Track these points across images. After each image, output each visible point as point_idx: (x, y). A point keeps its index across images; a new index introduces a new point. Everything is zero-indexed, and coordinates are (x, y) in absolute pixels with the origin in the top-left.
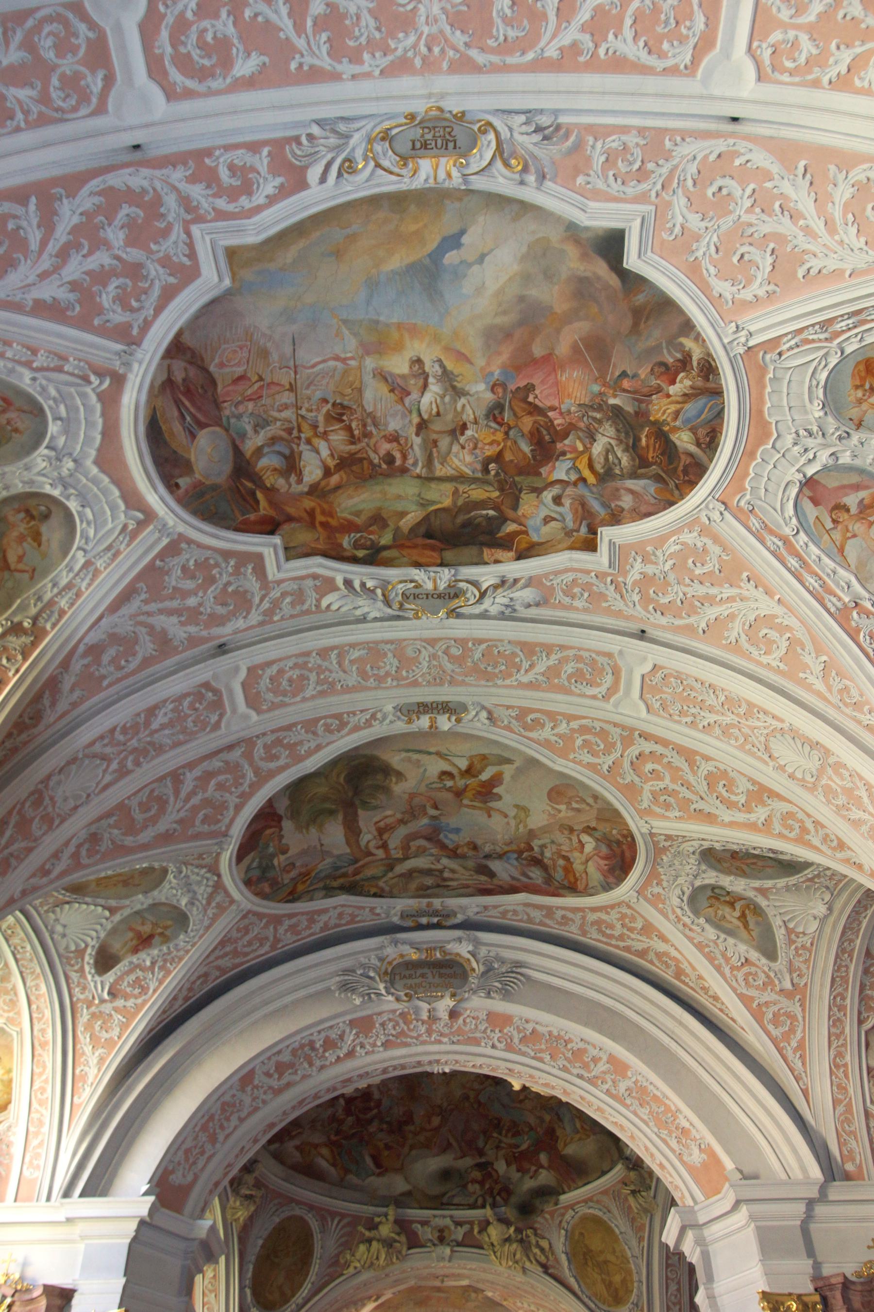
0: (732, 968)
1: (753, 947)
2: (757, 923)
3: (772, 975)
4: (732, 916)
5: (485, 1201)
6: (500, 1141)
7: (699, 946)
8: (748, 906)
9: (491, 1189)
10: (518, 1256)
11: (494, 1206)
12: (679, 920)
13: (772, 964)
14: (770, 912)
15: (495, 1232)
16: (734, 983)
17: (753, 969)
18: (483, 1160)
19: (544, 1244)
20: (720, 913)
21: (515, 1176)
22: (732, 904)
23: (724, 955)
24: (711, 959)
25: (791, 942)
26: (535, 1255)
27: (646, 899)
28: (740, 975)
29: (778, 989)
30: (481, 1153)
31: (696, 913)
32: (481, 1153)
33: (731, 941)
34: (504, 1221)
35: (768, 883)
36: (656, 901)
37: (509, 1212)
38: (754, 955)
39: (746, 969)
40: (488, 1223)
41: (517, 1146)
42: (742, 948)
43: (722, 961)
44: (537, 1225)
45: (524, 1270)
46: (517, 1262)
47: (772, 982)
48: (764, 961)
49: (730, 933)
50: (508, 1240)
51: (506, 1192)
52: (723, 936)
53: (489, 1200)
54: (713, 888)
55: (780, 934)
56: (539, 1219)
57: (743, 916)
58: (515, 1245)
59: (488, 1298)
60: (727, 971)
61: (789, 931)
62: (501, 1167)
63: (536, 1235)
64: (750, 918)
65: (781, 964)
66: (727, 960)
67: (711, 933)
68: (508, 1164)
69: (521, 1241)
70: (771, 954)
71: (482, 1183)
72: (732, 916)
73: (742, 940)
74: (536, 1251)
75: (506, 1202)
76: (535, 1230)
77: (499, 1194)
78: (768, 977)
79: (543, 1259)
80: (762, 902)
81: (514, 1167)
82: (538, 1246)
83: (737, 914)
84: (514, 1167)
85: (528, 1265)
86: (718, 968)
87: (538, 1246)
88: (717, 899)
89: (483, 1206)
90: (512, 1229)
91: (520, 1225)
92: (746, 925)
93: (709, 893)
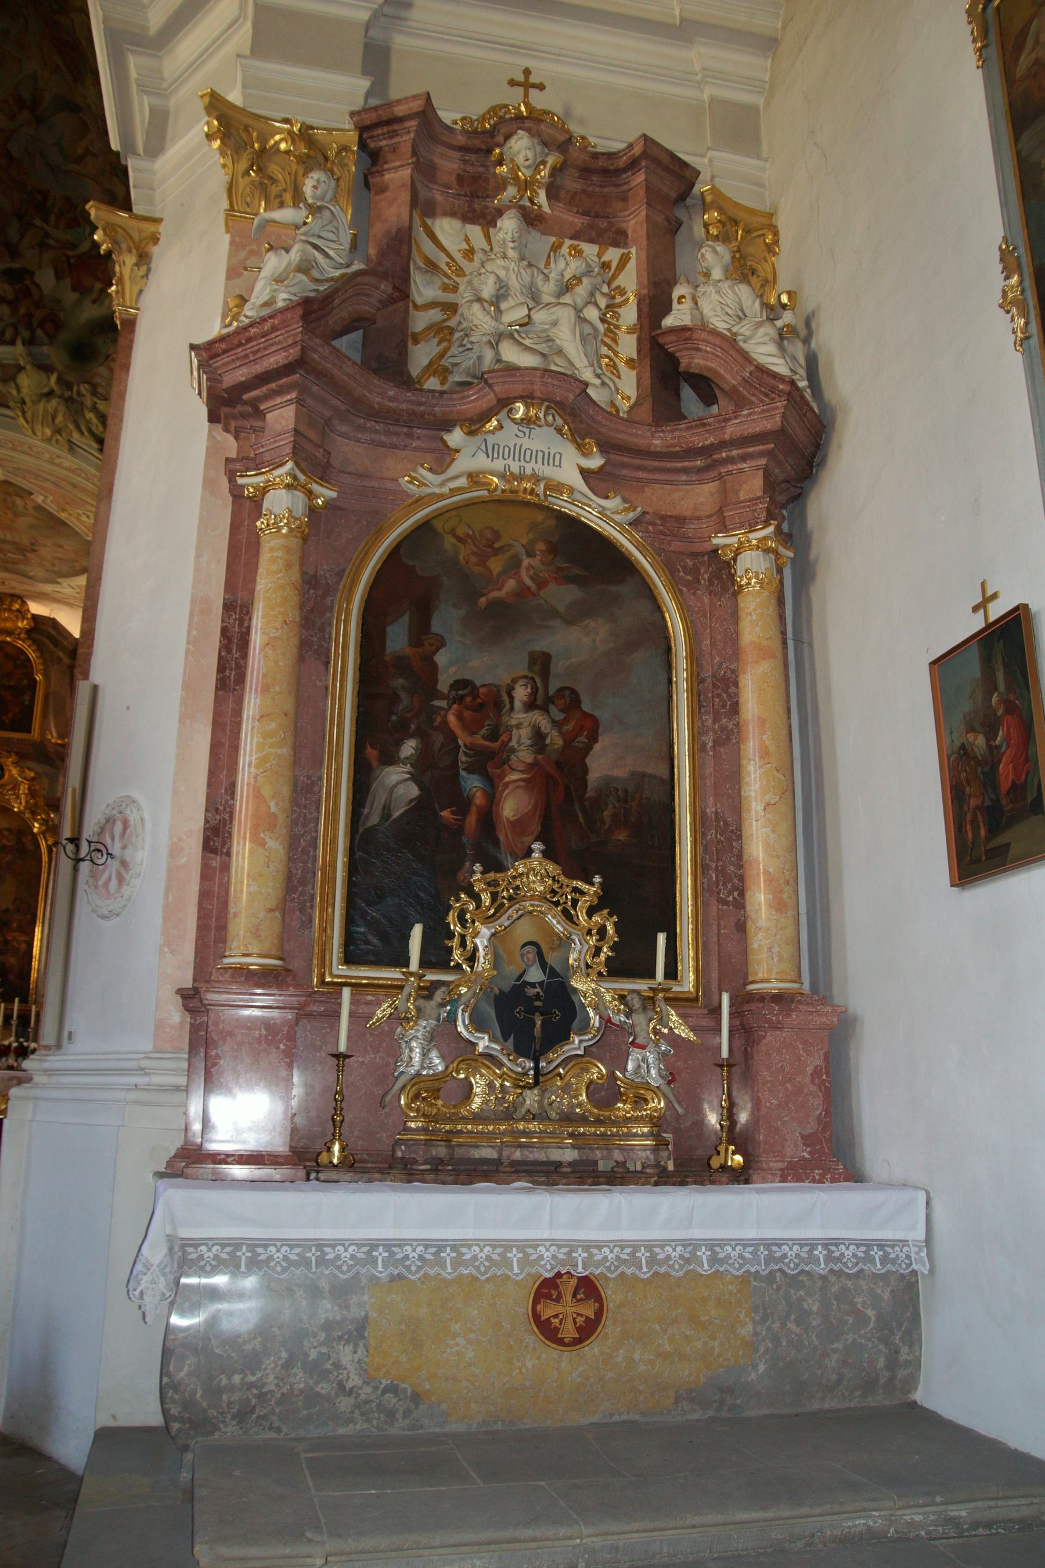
5: (17, 333)
6: (47, 235)
9: (29, 316)
10: (60, 419)
11: (29, 343)
15: (28, 382)
18: (16, 265)
19: (101, 406)
21: (70, 297)
26: (88, 422)
30: (14, 252)
32: (14, 252)
34: (46, 368)
37: (54, 354)
40: (20, 369)
41: (74, 246)
44: (98, 380)
45: (71, 447)
46: (58, 431)
50: (50, 394)
51: (53, 324)
53: (26, 334)
56: (103, 370)
58: (54, 402)
59: (39, 508)
62: (46, 279)
63: (94, 393)
68: (59, 277)
69: (69, 401)
71: (13, 304)
74: (90, 415)
75: (51, 338)
76: (94, 386)
77: (41, 325)
79: (98, 428)
81: (68, 282)
82: (95, 409)
84: (68, 282)
85: (76, 437)
87: (95, 409)
89: (13, 343)
90: (53, 378)
91: (71, 377)
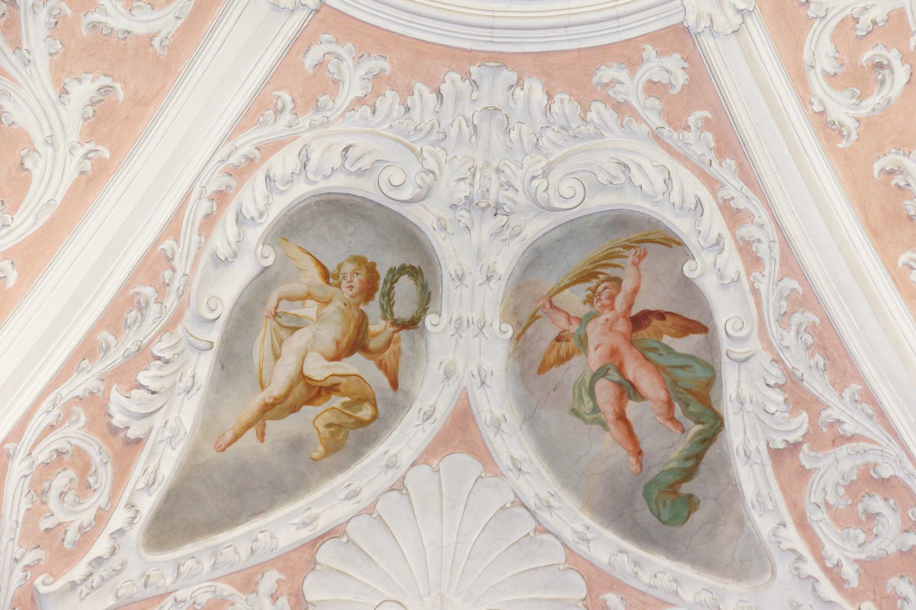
0: (96, 404)
1: (195, 451)
2: (297, 444)
3: (101, 547)
4: (310, 349)
7: (154, 265)
8: (364, 398)
12: (240, 172)
13: (136, 533)
14: (369, 472)
16: (39, 422)
17: (104, 476)
20: (310, 309)
22: (357, 342)
23: (142, 356)
24: (115, 318)
25: (247, 581)
27: (301, 41)
28: (74, 434)
29: (43, 585)
31: (289, 228)
33: (203, 366)
35: (511, 444)
36: (299, 85)
38: (163, 463)
39: (94, 449)
42: (186, 413)
43: (116, 357)
47: (64, 557)
48: (148, 504)
49: (231, 359)
52: (215, 335)
54: (421, 273)
55: (281, 528)
57: (317, 392)
60: (83, 382)
61: (301, 560)
64: (310, 420)
65: (141, 568)
66: (124, 376)
67: (229, 288)
70: (178, 519)
72: (310, 349)
73: (210, 408)
78: (87, 536)
80: (406, 439)
83: (319, 369)
86: (87, 350)
88: (368, 291)
92: (272, 409)
93: (386, 261)
